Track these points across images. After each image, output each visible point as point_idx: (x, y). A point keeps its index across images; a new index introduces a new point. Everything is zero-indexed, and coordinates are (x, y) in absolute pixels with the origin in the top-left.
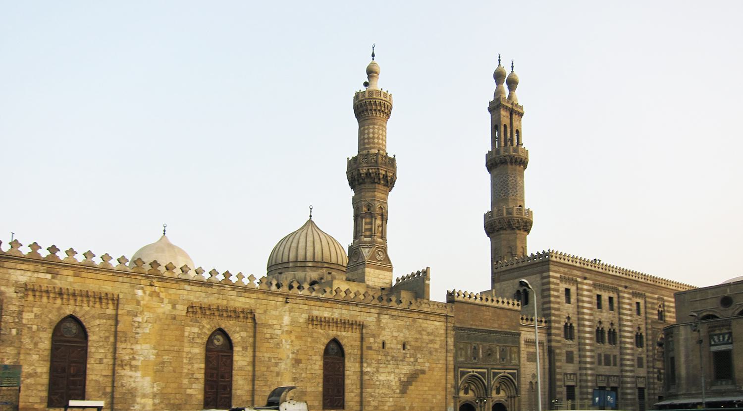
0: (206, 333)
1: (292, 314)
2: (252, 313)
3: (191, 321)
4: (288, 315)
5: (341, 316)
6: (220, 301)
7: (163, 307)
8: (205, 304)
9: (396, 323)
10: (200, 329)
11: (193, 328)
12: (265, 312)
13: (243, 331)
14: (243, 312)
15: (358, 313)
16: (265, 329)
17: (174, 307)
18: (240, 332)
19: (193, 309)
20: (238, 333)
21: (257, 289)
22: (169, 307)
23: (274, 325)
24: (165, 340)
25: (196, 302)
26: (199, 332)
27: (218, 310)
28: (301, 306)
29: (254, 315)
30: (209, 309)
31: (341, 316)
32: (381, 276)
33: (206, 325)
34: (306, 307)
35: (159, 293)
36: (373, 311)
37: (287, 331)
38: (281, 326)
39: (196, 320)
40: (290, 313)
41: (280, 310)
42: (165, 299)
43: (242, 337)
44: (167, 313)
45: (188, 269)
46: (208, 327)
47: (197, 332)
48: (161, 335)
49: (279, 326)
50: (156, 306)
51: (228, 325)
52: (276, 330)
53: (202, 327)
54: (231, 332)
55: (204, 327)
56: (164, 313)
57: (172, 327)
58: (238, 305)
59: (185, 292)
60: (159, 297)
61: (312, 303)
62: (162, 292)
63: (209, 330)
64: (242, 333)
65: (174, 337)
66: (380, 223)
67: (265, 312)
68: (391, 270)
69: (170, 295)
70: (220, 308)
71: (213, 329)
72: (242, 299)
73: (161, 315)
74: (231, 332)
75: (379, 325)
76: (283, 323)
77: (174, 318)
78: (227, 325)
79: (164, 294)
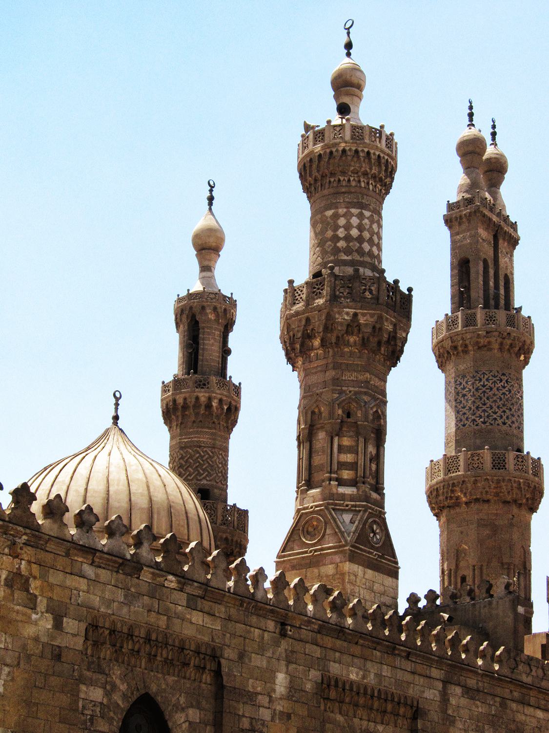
0: (118, 705)
1: (292, 667)
2: (215, 656)
3: (88, 670)
4: (284, 669)
5: (380, 683)
6: (153, 618)
7: (36, 623)
8: (123, 623)
9: (474, 708)
10: (107, 694)
11: (92, 688)
12: (242, 656)
13: (192, 706)
14: (198, 652)
15: (408, 677)
16: (241, 705)
17: (58, 625)
18: (188, 707)
19: (104, 636)
20: (183, 709)
21: (229, 591)
22: (47, 623)
23: (257, 694)
24: (38, 718)
25: (105, 616)
26: (105, 701)
27: (148, 640)
28: (309, 648)
29: (219, 664)
30: (130, 635)
31: (380, 683)
32: (376, 587)
33: (118, 682)
34: (317, 652)
35: (27, 580)
36: (435, 673)
37: (281, 713)
38: (271, 701)
39: (99, 666)
40: (287, 666)
41: (269, 654)
42: (40, 598)
43: (190, 723)
44: (44, 639)
45: (93, 519)
46: (123, 687)
47: (99, 700)
48: (28, 703)
49: (267, 699)
50: (18, 618)
51: (164, 687)
52: (261, 709)
53: (110, 689)
54: (170, 708)
55: (114, 687)
56: (36, 639)
57: (54, 681)
58: (189, 631)
59: (83, 584)
60: (27, 590)
61: (328, 641)
62: (35, 578)
63: (125, 696)
64: (191, 711)
65: (57, 711)
66: (374, 452)
67: (242, 656)
68: (394, 573)
69: (51, 586)
70: (154, 637)
71: (132, 694)
72: (197, 618)
73: (31, 644)
74: (170, 708)
75: (446, 713)
76: (274, 691)
77: (57, 655)
78: (163, 685)
79: (38, 583)
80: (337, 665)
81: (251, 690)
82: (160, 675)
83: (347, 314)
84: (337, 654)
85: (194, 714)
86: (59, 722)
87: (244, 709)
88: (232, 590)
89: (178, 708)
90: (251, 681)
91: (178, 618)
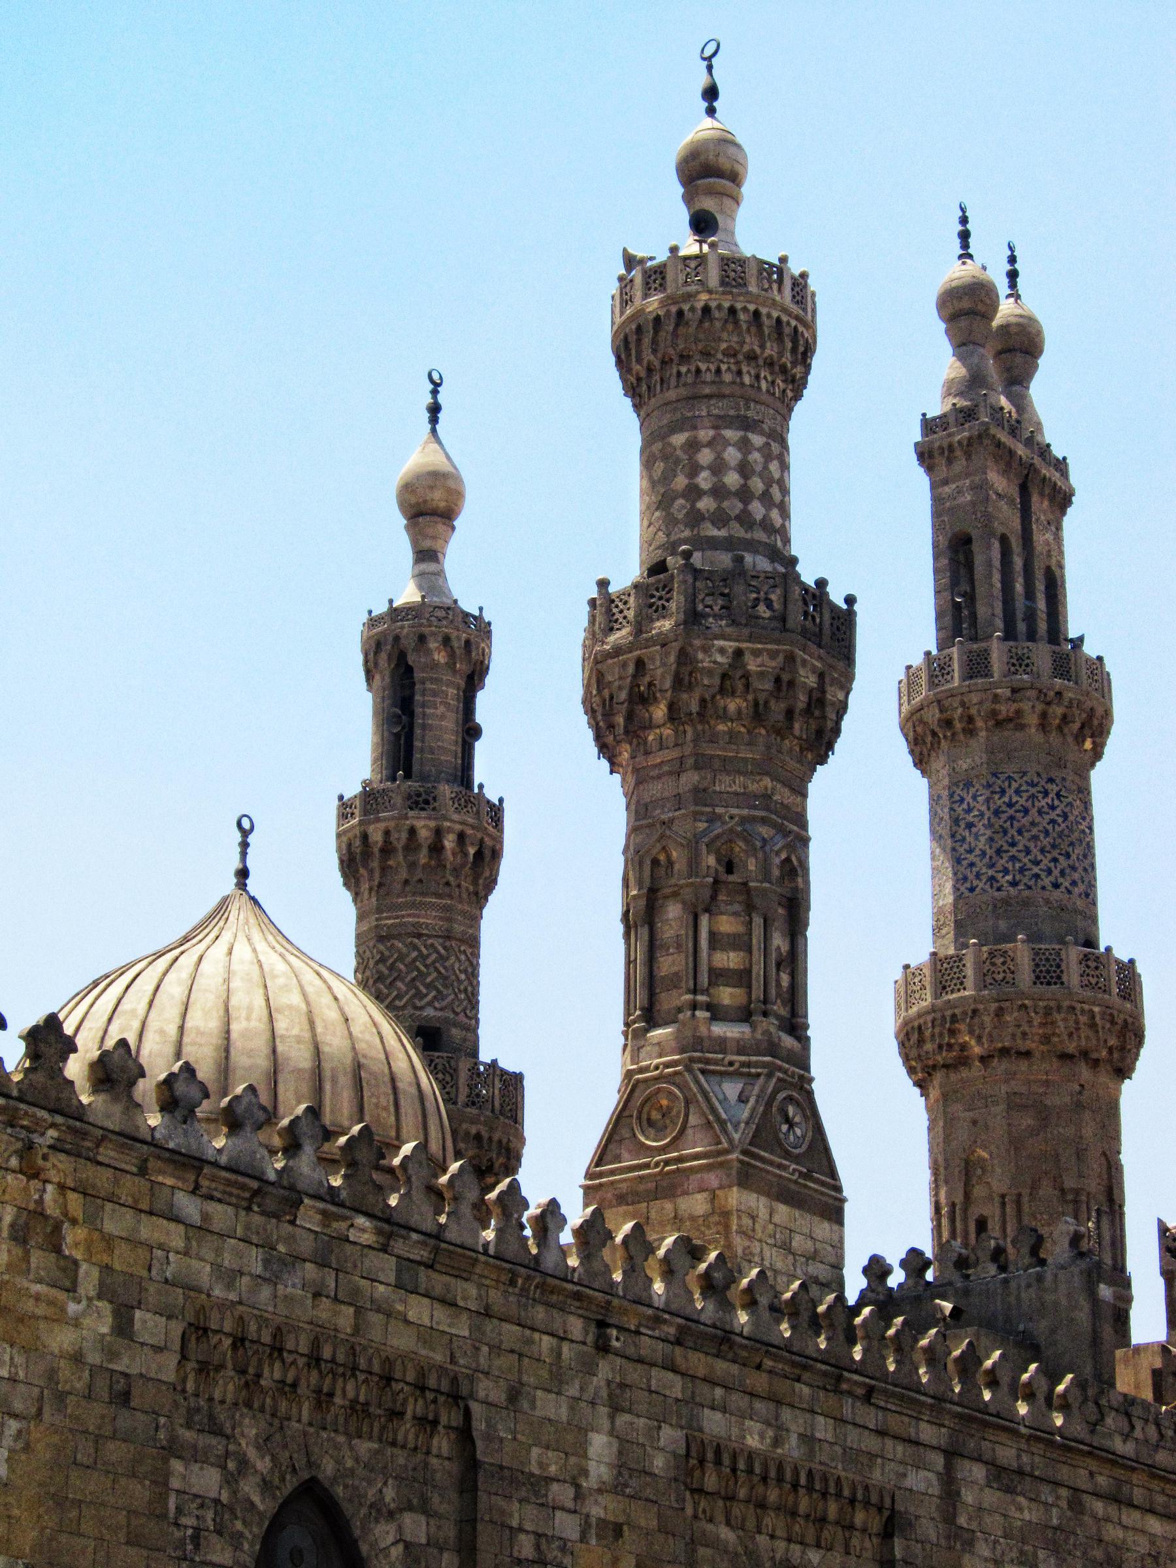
0: (252, 1504)
1: (623, 1419)
3: (188, 1426)
4: (605, 1424)
5: (811, 1453)
6: (324, 1311)
8: (262, 1321)
10: (230, 1480)
12: (514, 1395)
13: (410, 1508)
15: (871, 1443)
17: (123, 1327)
18: (401, 1510)
20: (391, 1515)
21: (486, 1253)
23: (549, 1480)
25: (224, 1306)
26: (225, 1497)
28: (660, 1378)
29: (467, 1414)
30: (277, 1349)
31: (811, 1453)
33: (252, 1453)
34: (675, 1387)
35: (57, 1227)
36: (927, 1432)
37: (602, 1522)
38: (579, 1496)
39: (211, 1417)
40: (612, 1418)
42: (84, 1267)
43: (408, 1546)
44: (94, 1358)
45: (195, 1093)
46: (263, 1465)
47: (213, 1494)
48: (60, 1502)
49: (570, 1492)
51: (349, 1463)
52: (558, 1514)
55: (244, 1464)
56: (77, 1358)
57: (115, 1451)
58: (401, 1341)
59: (175, 1236)
60: (57, 1250)
61: (698, 1362)
62: (74, 1222)
63: (266, 1486)
64: (408, 1519)
65: (122, 1518)
67: (514, 1395)
69: (109, 1241)
70: (327, 1353)
71: (283, 1479)
72: (419, 1310)
73: (65, 1370)
76: (585, 1473)
79: (81, 1233)
80: (718, 1416)
81: (537, 1472)
82: (341, 1439)
83: (722, 651)
84: (719, 1392)
85: (416, 1527)
86: (128, 1543)
87: (521, 1514)
88: (492, 1251)
89: (382, 1512)
90: (535, 1451)
91: (378, 1311)
